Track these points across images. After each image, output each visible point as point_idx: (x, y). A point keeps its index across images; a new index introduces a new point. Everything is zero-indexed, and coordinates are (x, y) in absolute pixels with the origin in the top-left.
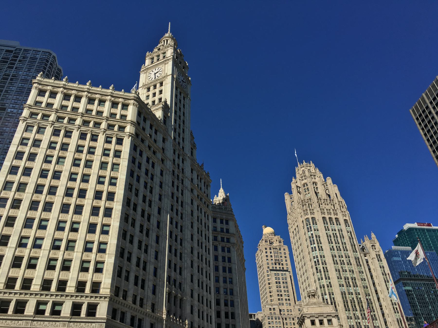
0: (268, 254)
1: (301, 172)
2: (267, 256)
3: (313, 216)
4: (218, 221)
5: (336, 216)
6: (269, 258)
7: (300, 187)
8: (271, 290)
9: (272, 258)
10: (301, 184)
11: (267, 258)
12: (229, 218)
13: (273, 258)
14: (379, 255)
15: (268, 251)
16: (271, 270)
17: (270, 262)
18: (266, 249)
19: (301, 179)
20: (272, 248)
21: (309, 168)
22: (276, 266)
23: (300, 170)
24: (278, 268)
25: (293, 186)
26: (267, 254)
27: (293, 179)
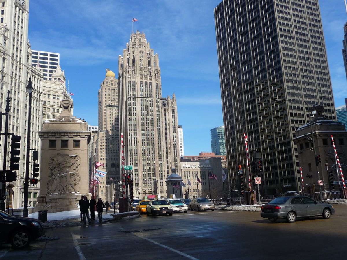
0: (108, 94)
2: (106, 95)
3: (134, 80)
4: (52, 97)
5: (150, 81)
6: (107, 97)
9: (109, 97)
12: (60, 94)
14: (174, 110)
15: (108, 91)
16: (107, 106)
17: (108, 99)
18: (106, 89)
20: (110, 89)
21: (140, 38)
22: (112, 103)
24: (113, 105)
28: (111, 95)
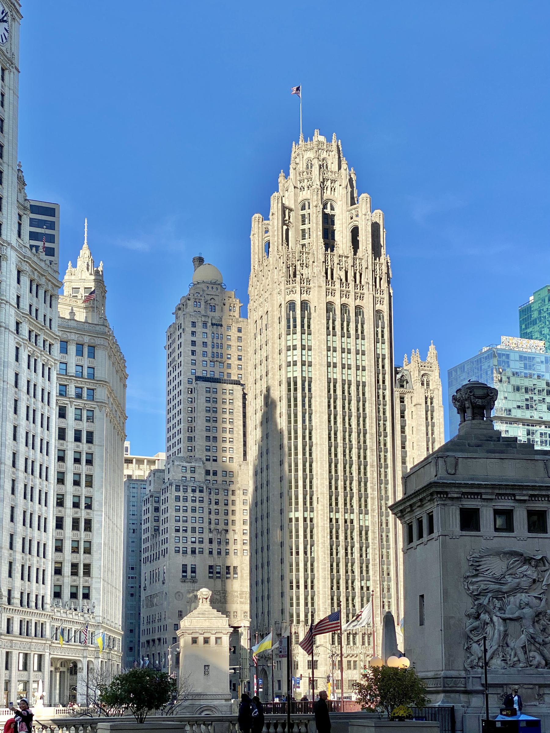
0: (199, 339)
1: (302, 167)
6: (199, 349)
7: (291, 210)
8: (194, 424)
9: (205, 349)
10: (295, 201)
11: (194, 348)
13: (209, 349)
15: (199, 329)
16: (198, 378)
17: (199, 357)
18: (194, 324)
19: (299, 186)
20: (209, 324)
23: (303, 155)
25: (275, 208)
26: (194, 339)
27: (281, 179)
28: (209, 344)
